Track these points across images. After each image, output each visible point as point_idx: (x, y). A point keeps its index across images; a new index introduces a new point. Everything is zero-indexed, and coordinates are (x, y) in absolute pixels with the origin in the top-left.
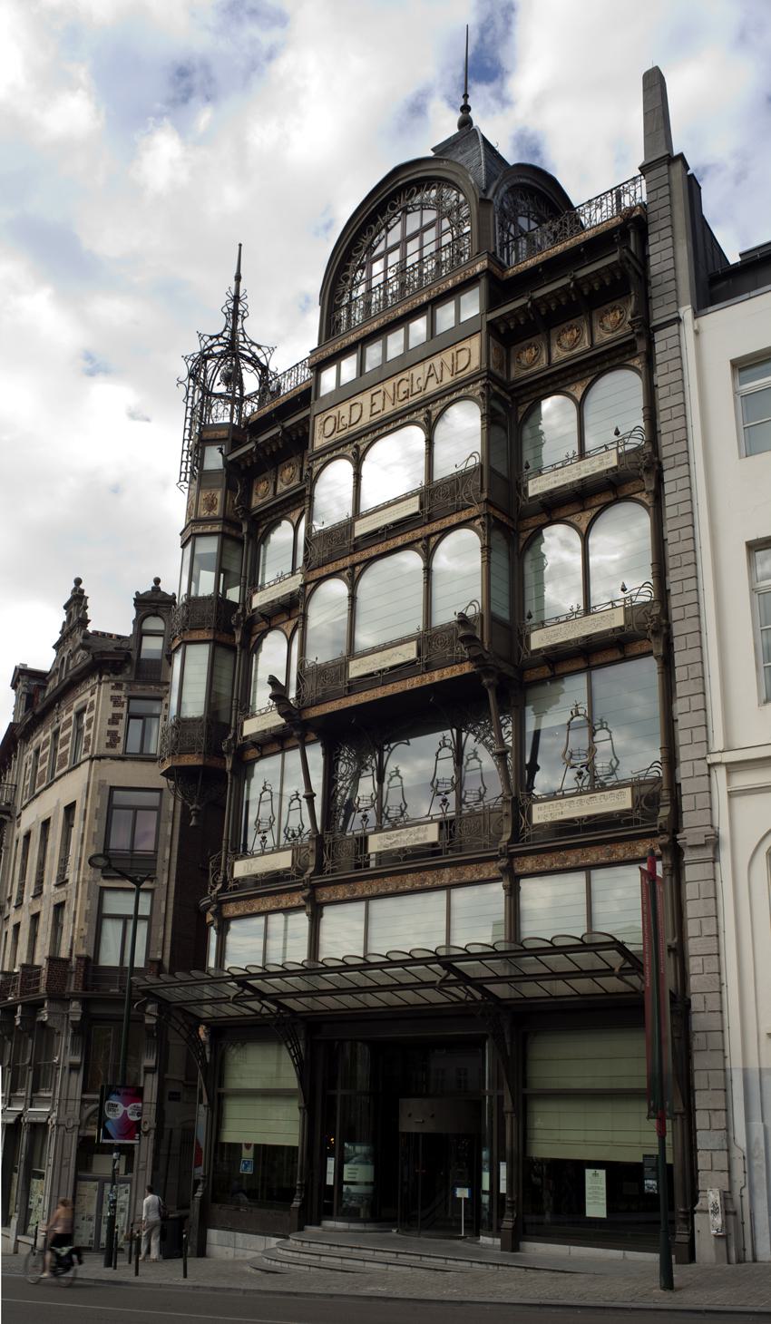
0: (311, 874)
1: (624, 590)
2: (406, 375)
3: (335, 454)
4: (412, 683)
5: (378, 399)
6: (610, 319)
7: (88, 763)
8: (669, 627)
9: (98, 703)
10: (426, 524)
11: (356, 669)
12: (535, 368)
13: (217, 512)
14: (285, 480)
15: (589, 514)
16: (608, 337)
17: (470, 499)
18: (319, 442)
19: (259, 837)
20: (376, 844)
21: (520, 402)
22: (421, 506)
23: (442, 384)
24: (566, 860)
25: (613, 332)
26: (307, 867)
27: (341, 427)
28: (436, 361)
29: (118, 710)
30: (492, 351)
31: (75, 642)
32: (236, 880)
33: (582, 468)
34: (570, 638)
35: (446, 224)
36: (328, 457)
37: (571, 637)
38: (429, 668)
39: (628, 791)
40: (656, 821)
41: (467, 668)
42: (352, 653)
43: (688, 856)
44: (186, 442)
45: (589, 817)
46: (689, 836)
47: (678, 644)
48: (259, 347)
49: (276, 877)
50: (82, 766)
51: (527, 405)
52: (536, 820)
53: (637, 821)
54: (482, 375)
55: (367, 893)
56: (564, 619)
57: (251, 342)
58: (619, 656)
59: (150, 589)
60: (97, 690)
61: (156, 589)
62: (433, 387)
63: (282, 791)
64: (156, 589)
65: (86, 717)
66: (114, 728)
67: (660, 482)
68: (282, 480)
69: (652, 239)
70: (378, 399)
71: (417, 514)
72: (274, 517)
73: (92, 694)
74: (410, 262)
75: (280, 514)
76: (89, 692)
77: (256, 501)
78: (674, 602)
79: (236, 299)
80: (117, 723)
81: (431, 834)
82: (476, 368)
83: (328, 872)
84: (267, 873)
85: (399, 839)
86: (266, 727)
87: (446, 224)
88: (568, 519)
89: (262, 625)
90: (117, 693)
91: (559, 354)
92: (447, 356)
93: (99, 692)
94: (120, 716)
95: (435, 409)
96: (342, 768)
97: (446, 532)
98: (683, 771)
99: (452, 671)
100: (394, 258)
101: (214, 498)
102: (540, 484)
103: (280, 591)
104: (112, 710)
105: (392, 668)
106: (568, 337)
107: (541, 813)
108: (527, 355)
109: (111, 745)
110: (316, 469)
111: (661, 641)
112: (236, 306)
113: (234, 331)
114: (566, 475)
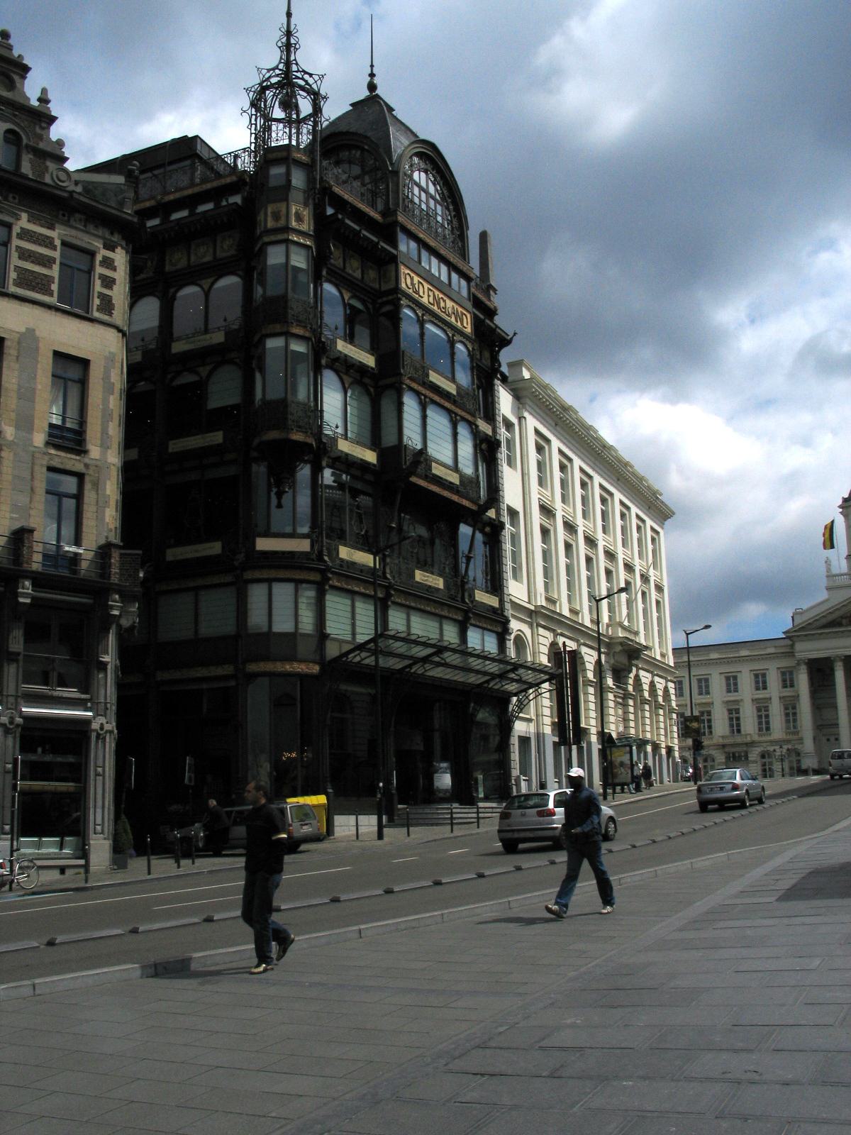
4: (455, 498)
28: (456, 306)
52: (477, 599)
62: (453, 320)
79: (289, 34)
86: (355, 454)
92: (460, 309)
97: (463, 419)
112: (288, 40)
113: (288, 64)
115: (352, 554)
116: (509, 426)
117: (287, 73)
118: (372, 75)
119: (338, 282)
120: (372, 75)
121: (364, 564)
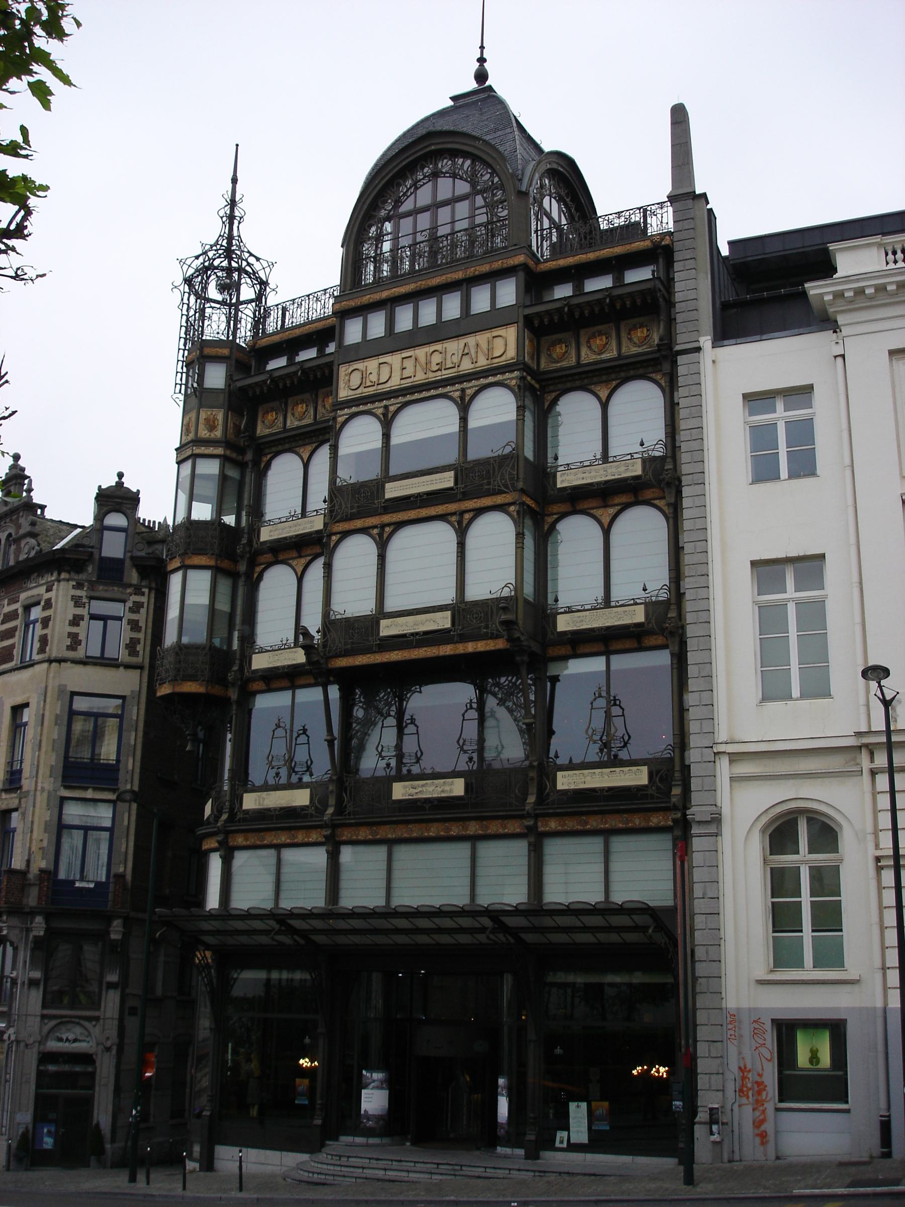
0: (332, 815)
1: (645, 590)
2: (438, 347)
3: (362, 408)
4: (446, 650)
5: (409, 364)
6: (640, 333)
7: (45, 665)
8: (683, 627)
9: (56, 602)
10: (460, 500)
11: (387, 628)
12: (564, 364)
13: (218, 433)
14: (297, 414)
15: (612, 511)
16: (634, 350)
17: (506, 486)
18: (344, 393)
19: (272, 773)
20: (400, 791)
21: (547, 390)
22: (456, 482)
23: (477, 365)
24: (586, 823)
25: (639, 347)
26: (326, 806)
27: (369, 384)
28: (471, 340)
29: (79, 611)
30: (527, 342)
31: (19, 527)
32: (247, 812)
33: (609, 471)
34: (594, 626)
35: (479, 200)
36: (354, 409)
37: (595, 625)
38: (463, 638)
39: (645, 769)
40: (670, 798)
41: (500, 644)
42: (381, 613)
43: (695, 830)
44: (181, 352)
45: (610, 789)
46: (696, 812)
47: (691, 644)
48: (258, 259)
49: (290, 813)
50: (36, 666)
51: (554, 395)
52: (560, 787)
53: (652, 797)
54: (518, 367)
55: (390, 836)
56: (589, 607)
57: (248, 252)
58: (636, 645)
59: (114, 484)
60: (55, 587)
61: (120, 484)
62: (466, 366)
63: (288, 725)
64: (120, 484)
65: (36, 613)
66: (75, 630)
67: (679, 493)
68: (293, 414)
69: (677, 266)
70: (409, 364)
71: (450, 489)
72: (280, 448)
73: (48, 590)
74: (442, 231)
75: (287, 446)
76: (45, 587)
77: (261, 430)
78: (688, 606)
79: (233, 203)
80: (78, 625)
81: (458, 788)
82: (512, 359)
83: (349, 814)
84: (282, 809)
85: (424, 789)
86: (278, 665)
87: (479, 200)
88: (593, 512)
89: (268, 557)
90: (78, 593)
91: (587, 356)
92: (482, 338)
93: (57, 590)
94: (81, 618)
95: (469, 388)
96: (359, 712)
98: (693, 755)
99: (487, 644)
100: (424, 221)
101: (215, 419)
102: (568, 478)
103: (293, 529)
104: (72, 610)
105: (426, 633)
106: (598, 342)
107: (565, 780)
108: (559, 350)
109: (72, 647)
110: (340, 420)
111: (677, 640)
112: (232, 210)
113: (230, 238)
114: (593, 474)
115: (264, 799)
116: (801, 394)
117: (229, 253)
118: (482, 60)
119: (293, 445)
120: (482, 60)
121: (284, 805)
